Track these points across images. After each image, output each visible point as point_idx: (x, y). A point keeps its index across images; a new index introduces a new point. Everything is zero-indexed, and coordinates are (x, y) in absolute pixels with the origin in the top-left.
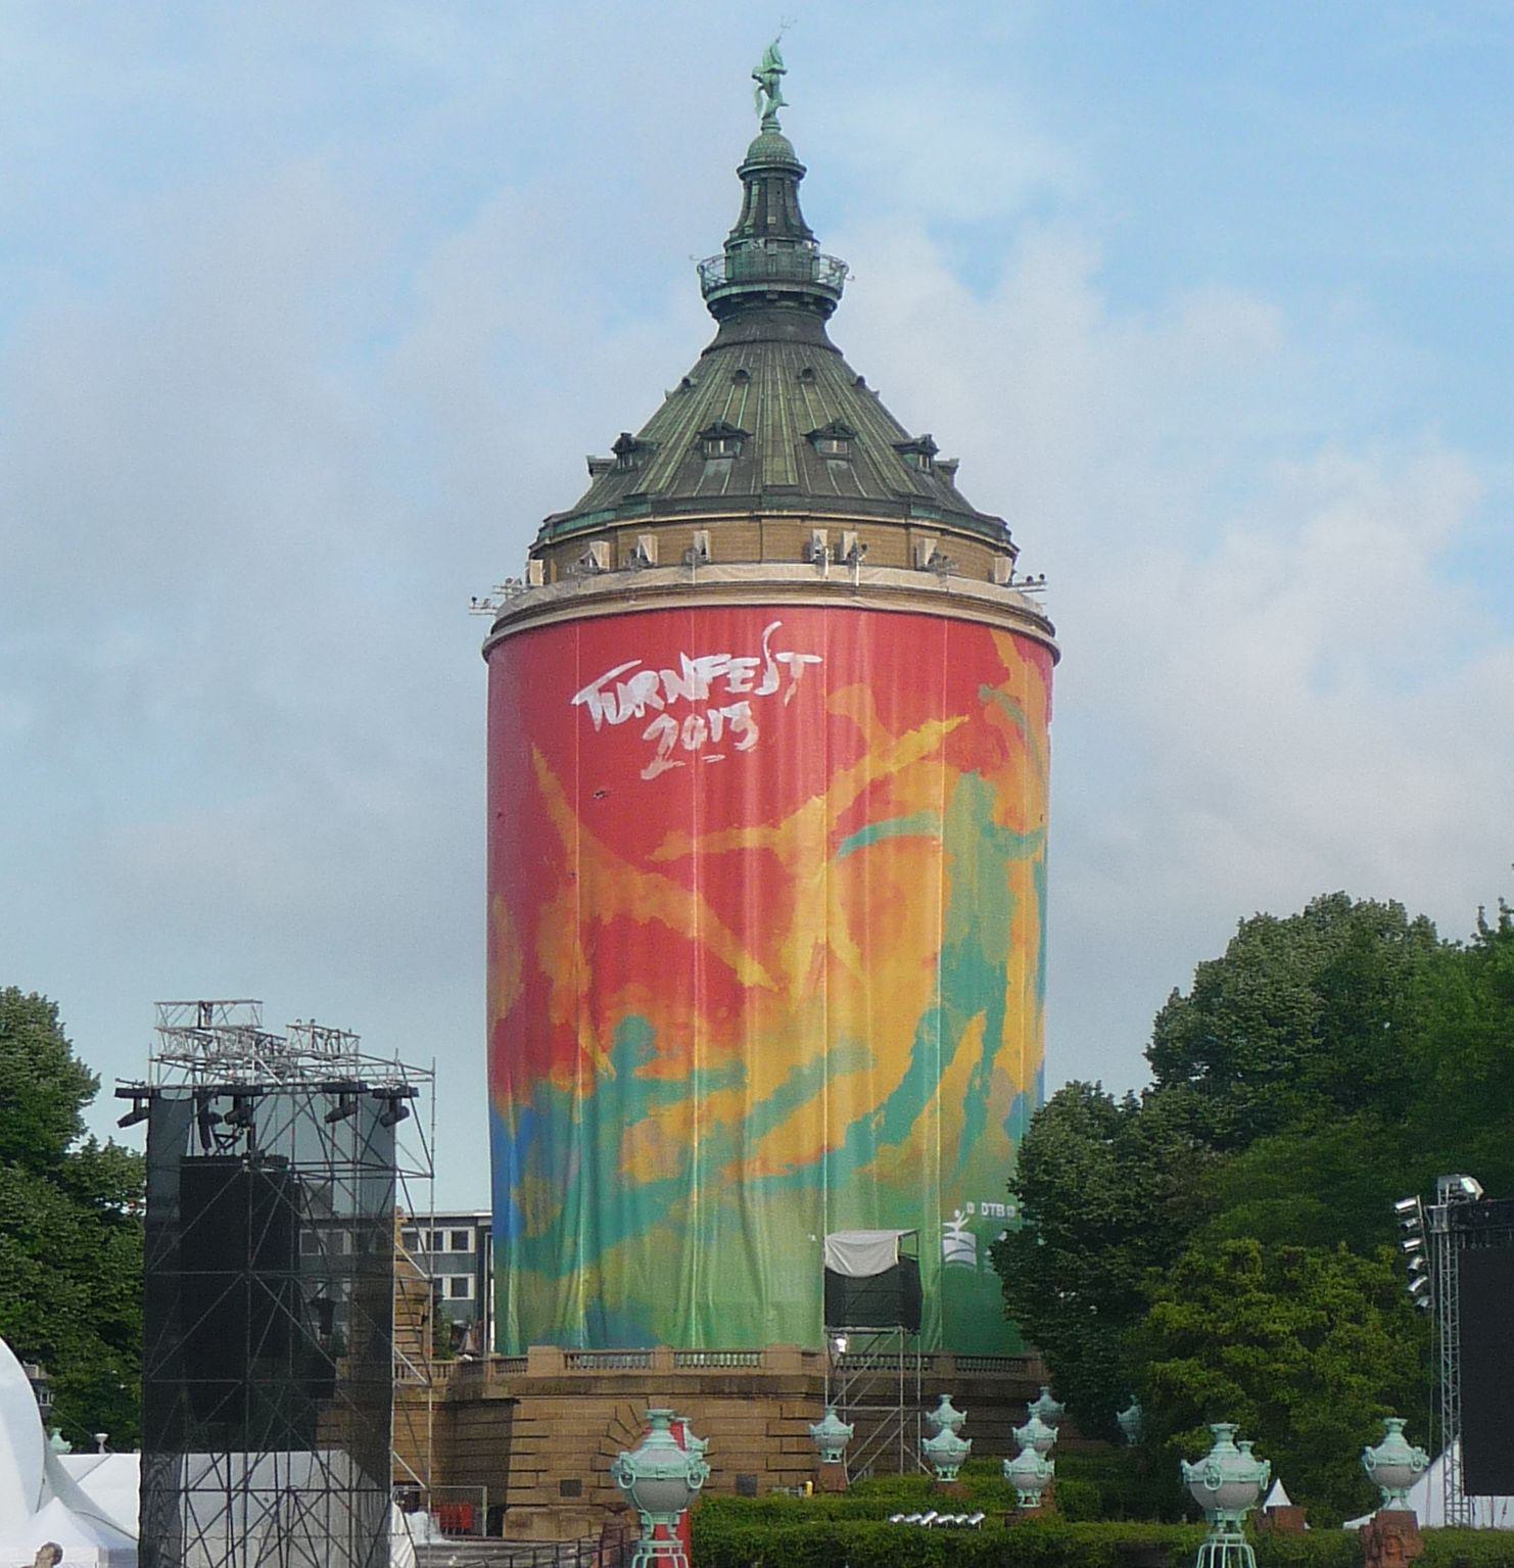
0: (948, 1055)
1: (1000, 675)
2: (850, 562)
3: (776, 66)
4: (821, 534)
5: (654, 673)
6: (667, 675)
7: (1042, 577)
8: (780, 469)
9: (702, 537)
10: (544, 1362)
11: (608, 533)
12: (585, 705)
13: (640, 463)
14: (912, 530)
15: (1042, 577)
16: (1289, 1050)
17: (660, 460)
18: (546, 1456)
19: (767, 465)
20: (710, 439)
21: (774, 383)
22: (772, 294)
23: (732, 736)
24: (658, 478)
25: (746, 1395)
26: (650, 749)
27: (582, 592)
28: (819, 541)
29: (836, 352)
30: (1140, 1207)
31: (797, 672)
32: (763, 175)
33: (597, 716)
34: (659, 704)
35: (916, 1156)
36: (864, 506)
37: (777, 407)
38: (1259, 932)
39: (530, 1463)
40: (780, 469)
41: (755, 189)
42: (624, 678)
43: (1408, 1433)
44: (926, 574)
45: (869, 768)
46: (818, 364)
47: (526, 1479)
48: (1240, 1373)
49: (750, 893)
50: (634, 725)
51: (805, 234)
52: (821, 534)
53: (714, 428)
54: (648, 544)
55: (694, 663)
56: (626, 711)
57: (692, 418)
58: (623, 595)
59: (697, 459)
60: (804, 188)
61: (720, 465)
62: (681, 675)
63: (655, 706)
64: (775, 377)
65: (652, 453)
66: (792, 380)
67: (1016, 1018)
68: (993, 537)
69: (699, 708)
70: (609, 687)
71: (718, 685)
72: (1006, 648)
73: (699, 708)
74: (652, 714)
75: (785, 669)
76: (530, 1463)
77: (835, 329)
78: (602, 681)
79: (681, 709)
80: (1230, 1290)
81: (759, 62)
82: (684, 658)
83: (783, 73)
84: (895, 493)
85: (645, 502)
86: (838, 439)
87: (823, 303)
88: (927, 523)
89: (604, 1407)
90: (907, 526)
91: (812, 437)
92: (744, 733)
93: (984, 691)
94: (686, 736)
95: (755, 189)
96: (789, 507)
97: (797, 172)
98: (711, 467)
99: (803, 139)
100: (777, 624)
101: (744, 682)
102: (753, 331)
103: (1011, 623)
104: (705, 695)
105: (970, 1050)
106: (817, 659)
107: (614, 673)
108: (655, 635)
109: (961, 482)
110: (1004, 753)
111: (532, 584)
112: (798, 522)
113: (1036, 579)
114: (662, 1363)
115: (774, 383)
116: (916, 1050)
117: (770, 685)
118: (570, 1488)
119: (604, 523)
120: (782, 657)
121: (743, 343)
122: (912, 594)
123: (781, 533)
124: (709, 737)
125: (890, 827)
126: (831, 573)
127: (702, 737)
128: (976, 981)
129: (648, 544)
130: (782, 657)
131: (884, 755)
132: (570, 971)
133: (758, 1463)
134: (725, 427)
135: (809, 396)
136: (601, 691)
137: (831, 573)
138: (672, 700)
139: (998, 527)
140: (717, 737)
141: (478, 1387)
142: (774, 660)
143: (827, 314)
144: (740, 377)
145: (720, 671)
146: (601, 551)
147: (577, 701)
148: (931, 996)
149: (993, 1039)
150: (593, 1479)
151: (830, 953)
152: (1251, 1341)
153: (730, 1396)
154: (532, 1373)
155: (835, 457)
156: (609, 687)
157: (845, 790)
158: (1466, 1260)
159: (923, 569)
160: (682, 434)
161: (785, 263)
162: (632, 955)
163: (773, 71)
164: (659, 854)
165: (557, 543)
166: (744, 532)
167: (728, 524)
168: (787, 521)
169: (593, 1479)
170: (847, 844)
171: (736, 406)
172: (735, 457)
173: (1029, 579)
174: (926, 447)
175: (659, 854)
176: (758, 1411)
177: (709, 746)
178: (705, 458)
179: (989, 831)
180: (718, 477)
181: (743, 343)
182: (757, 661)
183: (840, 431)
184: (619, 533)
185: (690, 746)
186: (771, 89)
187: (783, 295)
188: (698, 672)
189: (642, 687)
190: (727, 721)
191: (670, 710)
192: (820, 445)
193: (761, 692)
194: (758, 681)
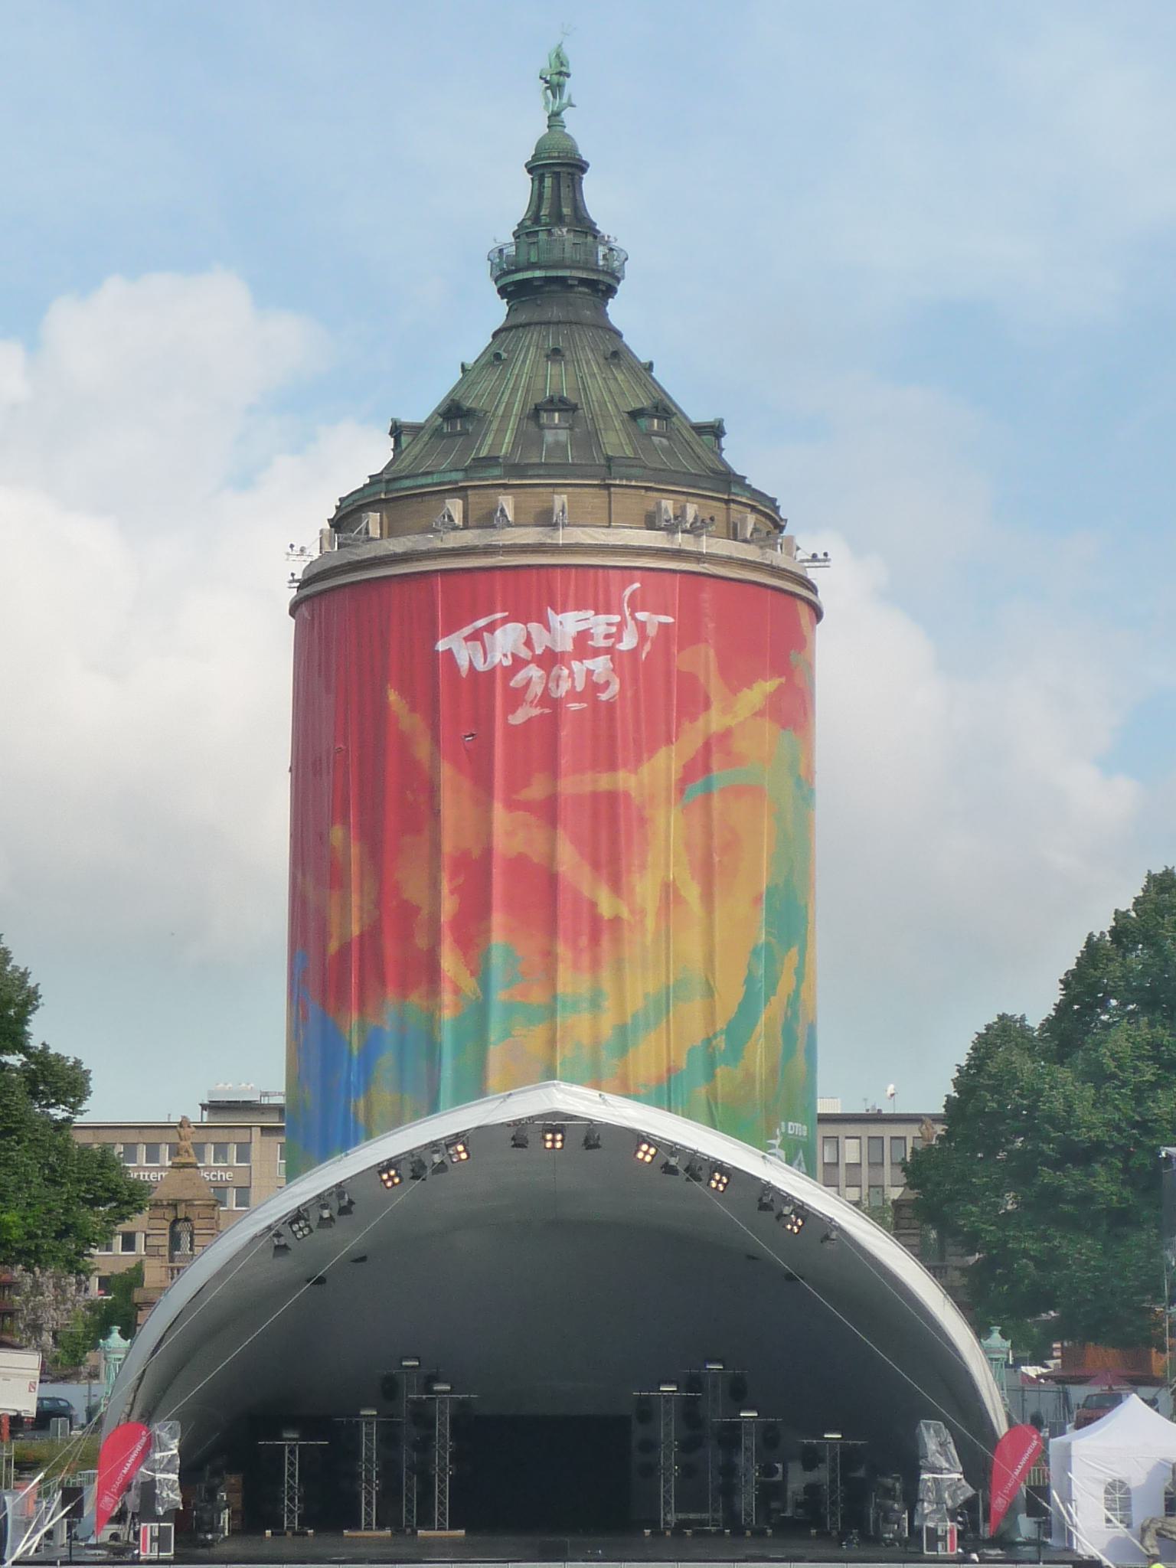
0: (772, 988)
3: (564, 69)
5: (521, 626)
6: (534, 627)
7: (826, 554)
8: (615, 441)
9: (560, 500)
11: (459, 491)
12: (449, 652)
13: (470, 428)
14: (733, 506)
15: (826, 554)
17: (495, 426)
20: (546, 411)
21: (588, 363)
22: (556, 277)
23: (594, 687)
26: (516, 698)
27: (440, 545)
28: (666, 511)
30: (1119, 1130)
31: (652, 631)
32: (557, 169)
33: (463, 662)
34: (524, 653)
41: (548, 182)
42: (491, 628)
43: (1001, 1333)
44: (752, 547)
49: (611, 833)
52: (668, 505)
53: (551, 400)
55: (559, 617)
57: (515, 390)
58: (489, 550)
59: (532, 427)
60: (589, 184)
61: (556, 432)
62: (548, 628)
63: (522, 655)
65: (480, 420)
66: (601, 361)
70: (476, 636)
71: (582, 637)
74: (518, 663)
75: (641, 627)
78: (467, 630)
79: (550, 660)
81: (543, 62)
83: (568, 75)
84: (713, 471)
85: (498, 465)
86: (658, 418)
88: (744, 500)
90: (727, 502)
91: (635, 415)
92: (607, 684)
94: (552, 685)
95: (548, 182)
96: (637, 479)
97: (581, 167)
98: (549, 436)
99: (584, 135)
100: (637, 585)
101: (607, 636)
104: (569, 647)
106: (670, 620)
107: (481, 623)
111: (371, 535)
112: (643, 492)
113: (821, 556)
115: (588, 363)
116: (750, 980)
117: (628, 643)
119: (456, 482)
120: (641, 616)
121: (548, 323)
123: (626, 501)
124: (573, 687)
126: (681, 540)
131: (727, 710)
134: (562, 400)
135: (620, 377)
136: (467, 639)
137: (681, 540)
138: (539, 651)
142: (634, 618)
144: (556, 354)
145: (582, 626)
146: (455, 507)
147: (441, 646)
151: (676, 890)
155: (657, 434)
156: (476, 636)
157: (690, 741)
159: (745, 541)
160: (509, 405)
163: (560, 73)
166: (593, 499)
167: (578, 490)
168: (632, 491)
170: (695, 789)
171: (557, 380)
172: (571, 428)
173: (814, 556)
177: (573, 695)
178: (541, 427)
180: (557, 443)
181: (548, 323)
182: (616, 618)
184: (469, 492)
186: (554, 85)
187: (583, 282)
188: (568, 624)
189: (507, 640)
190: (590, 673)
192: (643, 422)
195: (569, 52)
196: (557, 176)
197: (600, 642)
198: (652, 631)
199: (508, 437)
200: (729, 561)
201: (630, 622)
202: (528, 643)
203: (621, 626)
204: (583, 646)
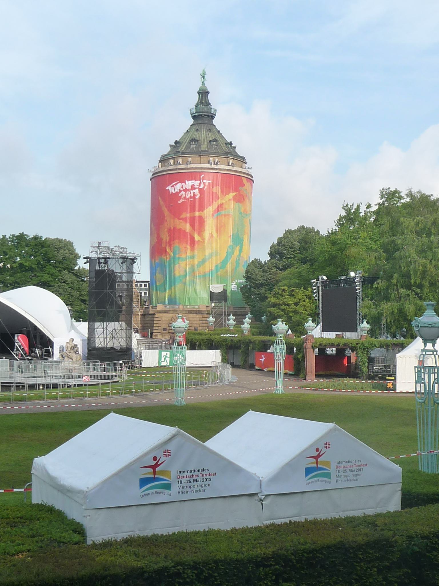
0: (233, 253)
1: (244, 185)
2: (217, 164)
4: (212, 159)
6: (183, 184)
8: (204, 147)
9: (190, 159)
10: (160, 307)
11: (173, 158)
16: (294, 253)
18: (160, 324)
19: (202, 146)
22: (203, 115)
24: (182, 148)
25: (196, 313)
29: (215, 126)
30: (266, 281)
31: (207, 184)
33: (171, 191)
34: (182, 189)
35: (227, 272)
36: (219, 154)
37: (204, 136)
38: (289, 232)
39: (158, 325)
40: (204, 147)
42: (176, 185)
43: (313, 321)
45: (220, 202)
46: (211, 128)
47: (157, 328)
48: (283, 310)
49: (198, 224)
50: (177, 193)
51: (209, 104)
52: (212, 159)
54: (180, 160)
56: (176, 191)
58: (176, 169)
64: (204, 131)
67: (245, 247)
68: (242, 160)
69: (189, 190)
70: (173, 186)
72: (244, 181)
73: (189, 190)
74: (180, 191)
75: (204, 183)
76: (158, 325)
77: (214, 121)
78: (172, 185)
79: (186, 190)
80: (282, 296)
81: (201, 73)
82: (186, 181)
87: (212, 117)
89: (171, 315)
91: (210, 141)
93: (240, 188)
97: (208, 93)
98: (192, 146)
102: (200, 122)
103: (245, 176)
104: (190, 188)
105: (237, 253)
106: (210, 182)
107: (174, 184)
108: (182, 177)
109: (236, 150)
110: (244, 199)
114: (181, 308)
116: (227, 252)
117: (202, 186)
118: (164, 329)
120: (204, 181)
122: (228, 170)
125: (223, 212)
126: (213, 166)
127: (189, 195)
128: (238, 240)
129: (180, 160)
130: (204, 181)
132: (165, 238)
133: (198, 325)
134: (194, 139)
135: (210, 134)
137: (213, 166)
139: (243, 158)
140: (192, 195)
141: (149, 311)
143: (213, 119)
146: (172, 161)
147: (167, 188)
148: (230, 243)
149: (241, 250)
150: (169, 328)
151: (212, 236)
152: (286, 305)
153: (193, 313)
154: (158, 309)
156: (173, 186)
157: (215, 205)
158: (324, 291)
161: (206, 109)
162: (176, 234)
164: (181, 217)
165: (164, 160)
166: (198, 158)
169: (169, 328)
170: (216, 215)
171: (196, 135)
174: (231, 144)
175: (181, 217)
176: (198, 316)
177: (191, 197)
179: (241, 213)
183: (215, 140)
185: (187, 197)
186: (204, 77)
187: (205, 115)
188: (189, 184)
189: (179, 186)
191: (183, 190)
192: (212, 143)
193: (200, 187)
194: (200, 186)
195: (206, 70)
196: (202, 95)
197: (196, 187)
198: (207, 184)
199: (184, 147)
200: (224, 170)
201: (202, 183)
202: (182, 187)
203: (200, 183)
204: (193, 187)
